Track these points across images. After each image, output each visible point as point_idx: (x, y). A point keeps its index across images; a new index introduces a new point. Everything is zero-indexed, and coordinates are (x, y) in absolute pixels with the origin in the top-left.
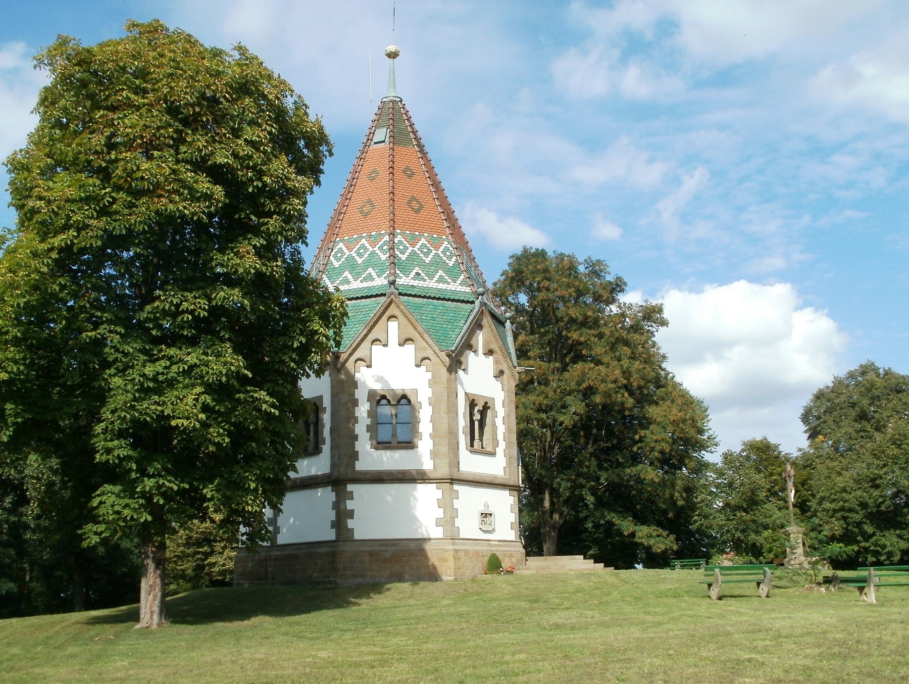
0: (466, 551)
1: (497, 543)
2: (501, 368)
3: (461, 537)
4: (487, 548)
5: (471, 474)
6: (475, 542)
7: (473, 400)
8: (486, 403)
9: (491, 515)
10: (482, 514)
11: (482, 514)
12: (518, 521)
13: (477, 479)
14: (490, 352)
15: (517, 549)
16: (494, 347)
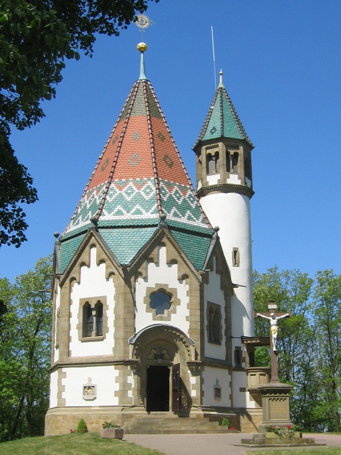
0: (64, 417)
1: (98, 408)
2: (111, 270)
3: (66, 405)
4: (85, 413)
5: (79, 358)
6: (77, 408)
7: (87, 303)
8: (99, 302)
9: (93, 387)
10: (85, 387)
11: (85, 387)
12: (122, 389)
13: (84, 361)
14: (101, 262)
15: (115, 412)
16: (104, 256)
